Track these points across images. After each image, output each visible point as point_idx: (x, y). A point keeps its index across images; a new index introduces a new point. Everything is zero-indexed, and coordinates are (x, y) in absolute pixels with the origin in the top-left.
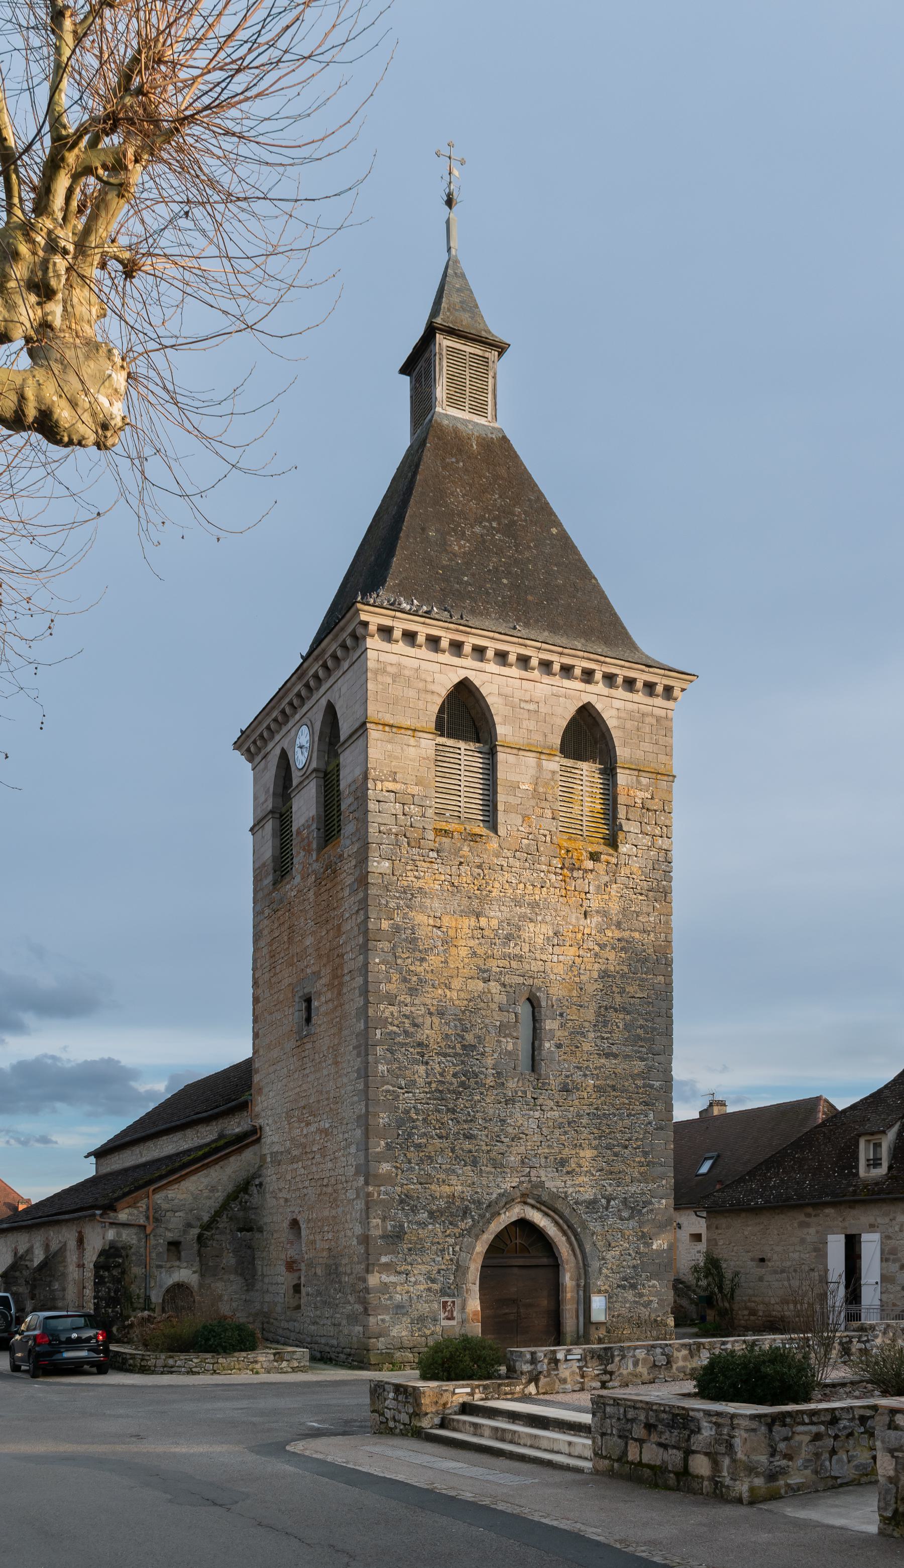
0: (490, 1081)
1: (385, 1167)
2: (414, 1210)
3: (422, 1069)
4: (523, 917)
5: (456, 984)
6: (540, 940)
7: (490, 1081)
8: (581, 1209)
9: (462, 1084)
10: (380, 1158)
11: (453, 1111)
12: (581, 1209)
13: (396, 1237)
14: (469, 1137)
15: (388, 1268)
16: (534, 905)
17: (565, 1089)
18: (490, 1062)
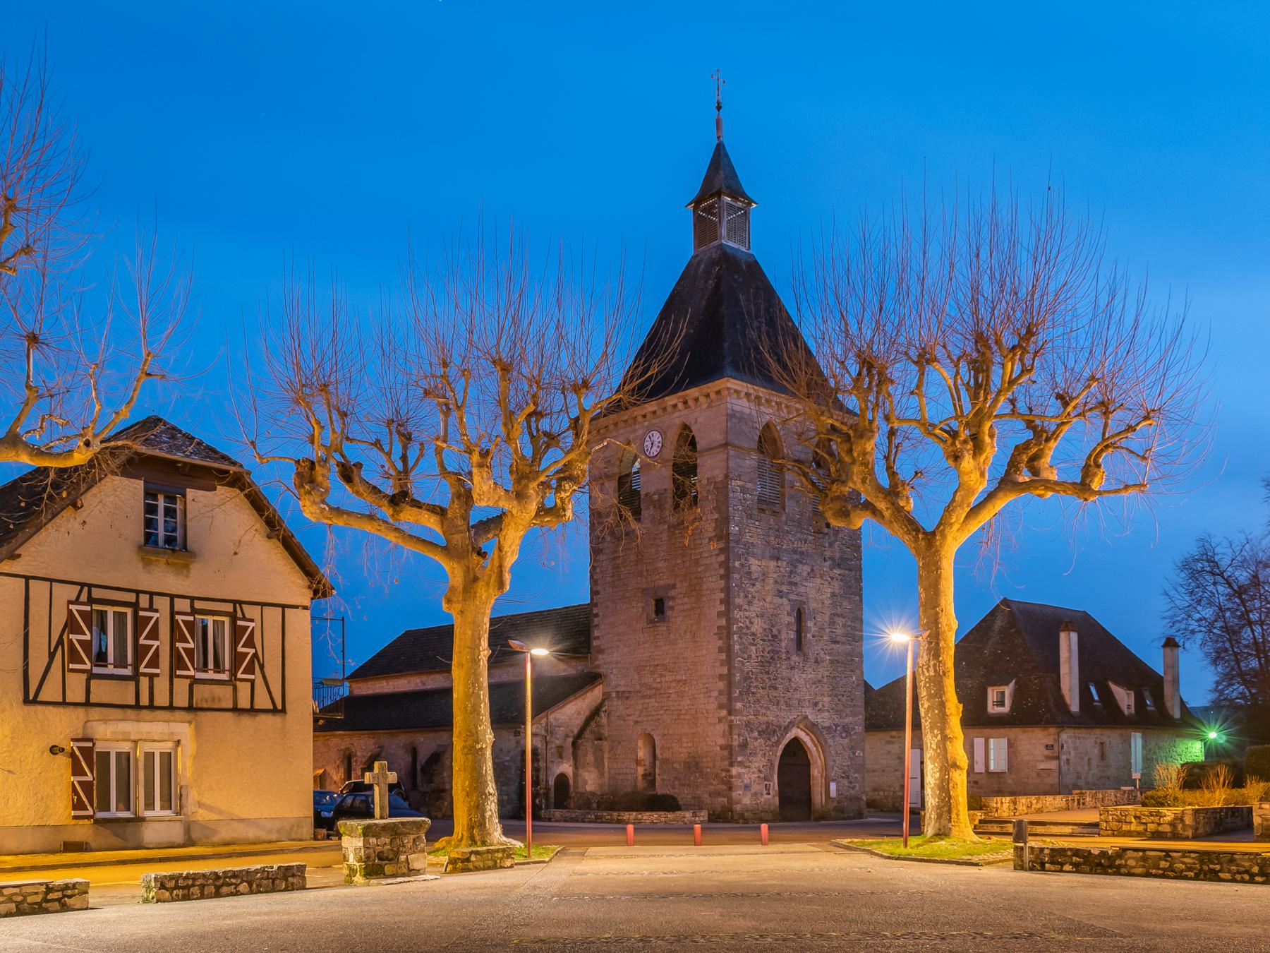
0: (784, 656)
1: (739, 705)
2: (752, 731)
3: (753, 648)
4: (798, 561)
5: (769, 599)
6: (805, 574)
7: (784, 656)
8: (825, 732)
9: (772, 658)
10: (737, 700)
11: (768, 673)
12: (825, 732)
13: (744, 746)
14: (776, 688)
15: (741, 764)
16: (802, 553)
17: (816, 662)
18: (783, 644)
